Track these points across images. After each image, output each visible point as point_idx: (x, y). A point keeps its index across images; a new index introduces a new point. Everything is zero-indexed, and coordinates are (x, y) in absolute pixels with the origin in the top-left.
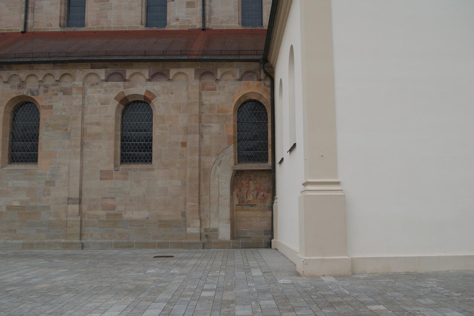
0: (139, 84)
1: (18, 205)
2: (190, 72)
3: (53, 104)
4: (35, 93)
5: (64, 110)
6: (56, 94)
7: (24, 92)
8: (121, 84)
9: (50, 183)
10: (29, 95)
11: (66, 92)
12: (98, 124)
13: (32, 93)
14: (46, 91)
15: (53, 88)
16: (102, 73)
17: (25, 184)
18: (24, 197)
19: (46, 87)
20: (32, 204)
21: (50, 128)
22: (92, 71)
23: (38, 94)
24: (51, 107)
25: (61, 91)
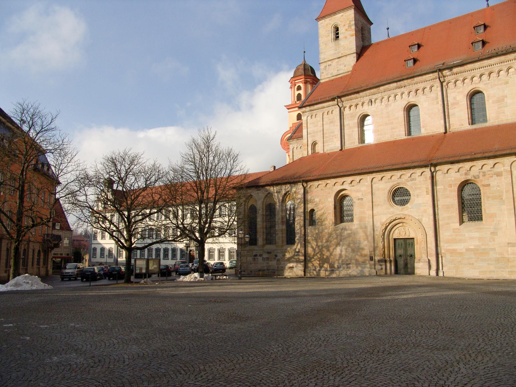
4: (477, 177)
7: (469, 177)
15: (489, 173)
23: (479, 178)
24: (489, 185)
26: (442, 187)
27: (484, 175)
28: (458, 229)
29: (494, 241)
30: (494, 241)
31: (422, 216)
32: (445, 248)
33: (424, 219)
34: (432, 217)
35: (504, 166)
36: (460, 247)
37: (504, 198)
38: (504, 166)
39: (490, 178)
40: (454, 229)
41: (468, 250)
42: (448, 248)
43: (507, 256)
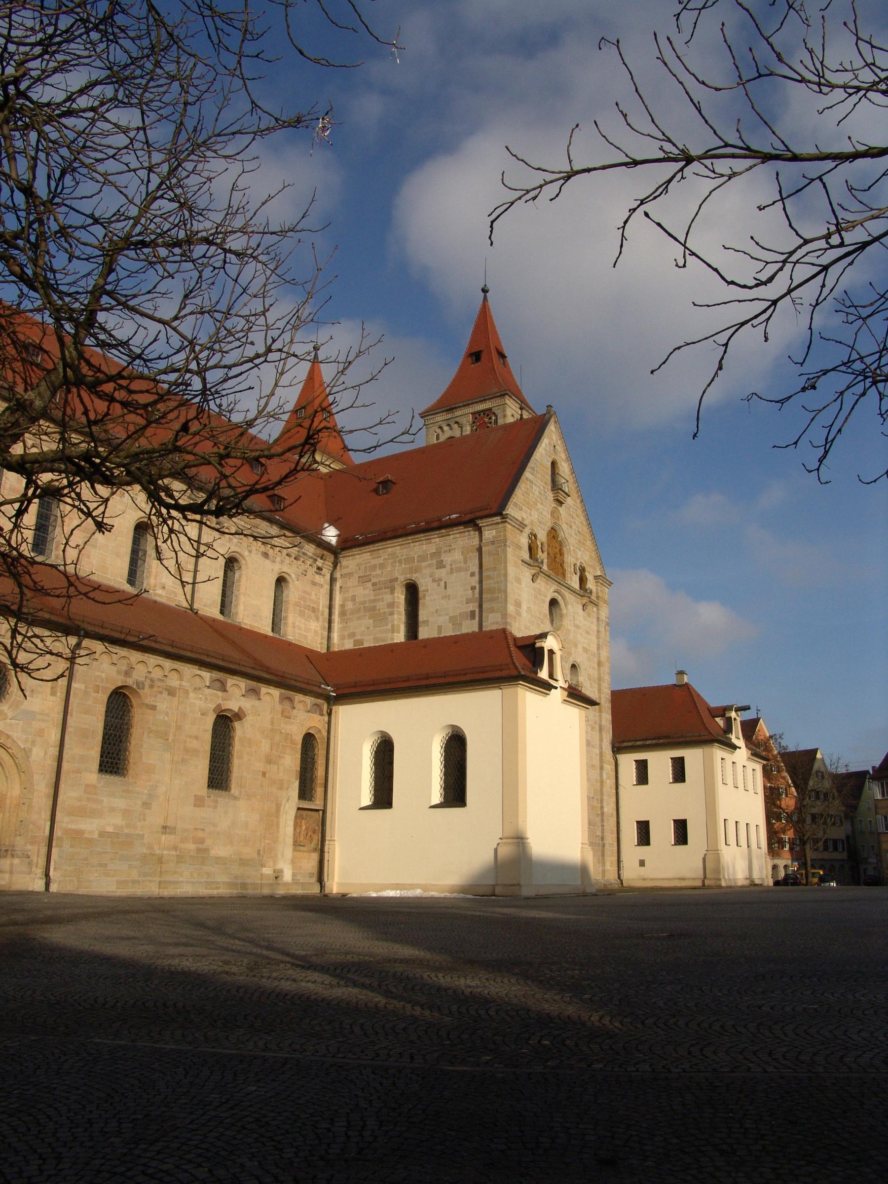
0: (236, 695)
1: (111, 830)
2: (276, 692)
3: (158, 704)
4: (141, 686)
5: (167, 714)
6: (161, 693)
7: (130, 682)
8: (220, 693)
9: (146, 805)
10: (135, 687)
11: (171, 692)
12: (196, 738)
13: (138, 684)
14: (151, 686)
15: (159, 684)
16: (207, 675)
17: (120, 803)
18: (118, 821)
19: (152, 680)
20: (126, 831)
21: (152, 735)
22: (199, 672)
23: (143, 688)
24: (154, 708)
25: (166, 689)
26: (83, 686)
27: (151, 686)
28: (94, 787)
29: (144, 820)
30: (144, 820)
31: (33, 743)
32: (64, 825)
33: (35, 751)
34: (54, 751)
35: (181, 679)
36: (90, 826)
37: (170, 740)
38: (181, 679)
39: (159, 695)
40: (87, 786)
41: (102, 834)
42: (69, 826)
43: (158, 852)
